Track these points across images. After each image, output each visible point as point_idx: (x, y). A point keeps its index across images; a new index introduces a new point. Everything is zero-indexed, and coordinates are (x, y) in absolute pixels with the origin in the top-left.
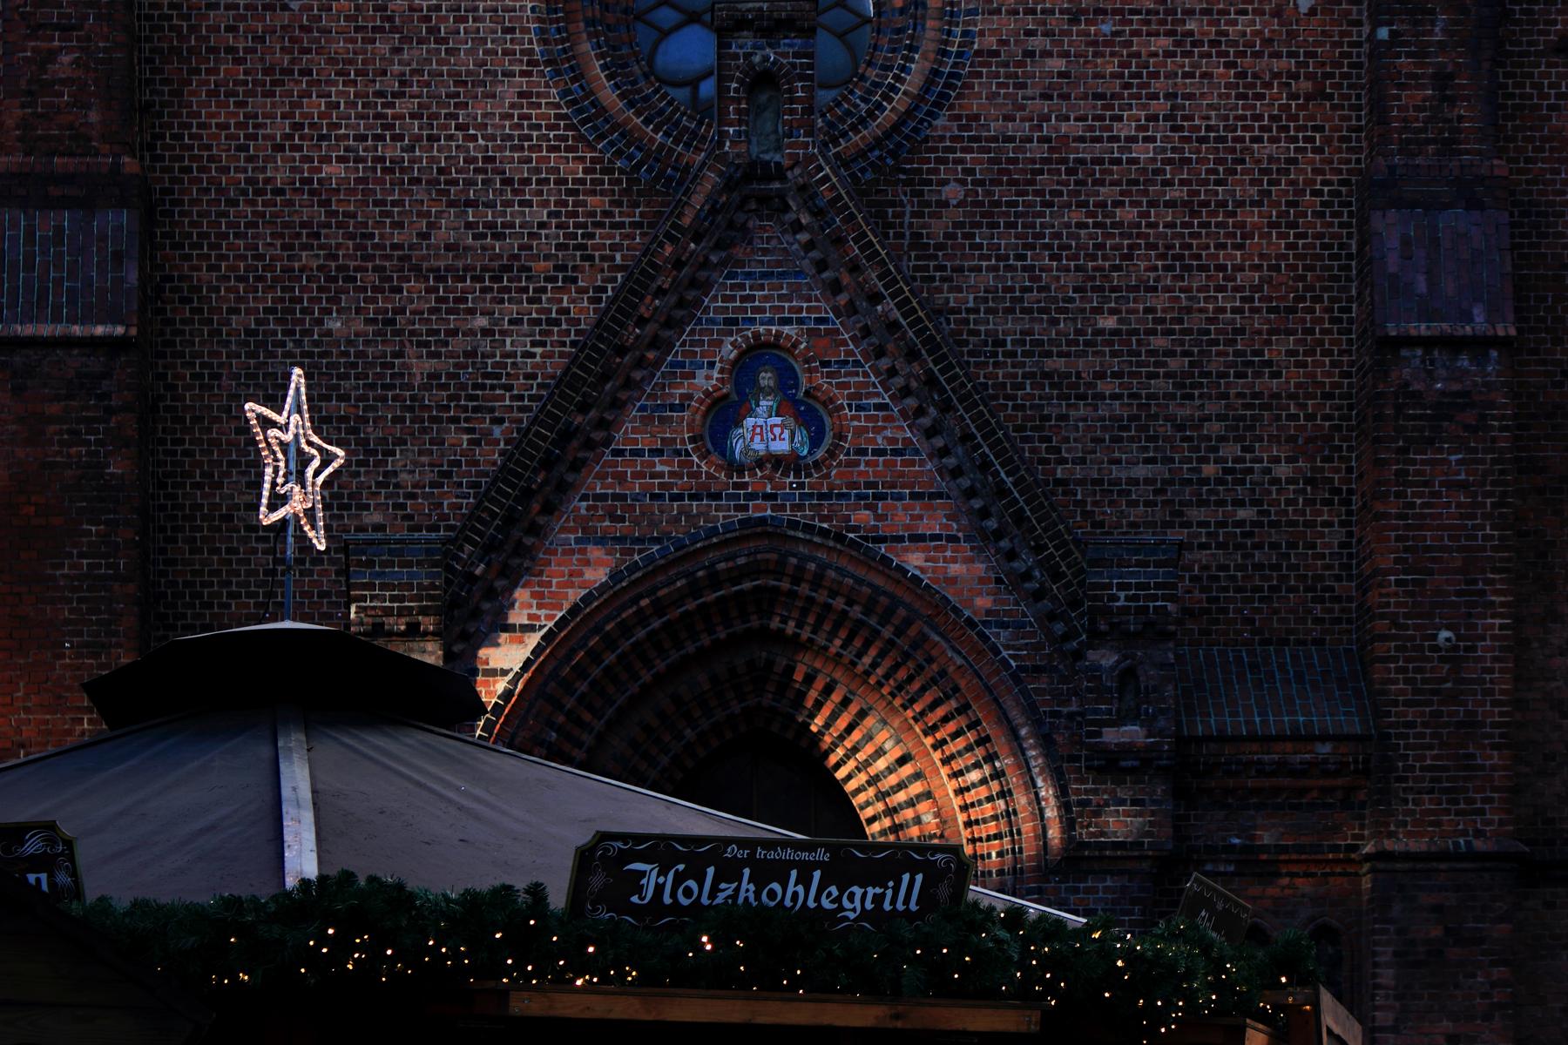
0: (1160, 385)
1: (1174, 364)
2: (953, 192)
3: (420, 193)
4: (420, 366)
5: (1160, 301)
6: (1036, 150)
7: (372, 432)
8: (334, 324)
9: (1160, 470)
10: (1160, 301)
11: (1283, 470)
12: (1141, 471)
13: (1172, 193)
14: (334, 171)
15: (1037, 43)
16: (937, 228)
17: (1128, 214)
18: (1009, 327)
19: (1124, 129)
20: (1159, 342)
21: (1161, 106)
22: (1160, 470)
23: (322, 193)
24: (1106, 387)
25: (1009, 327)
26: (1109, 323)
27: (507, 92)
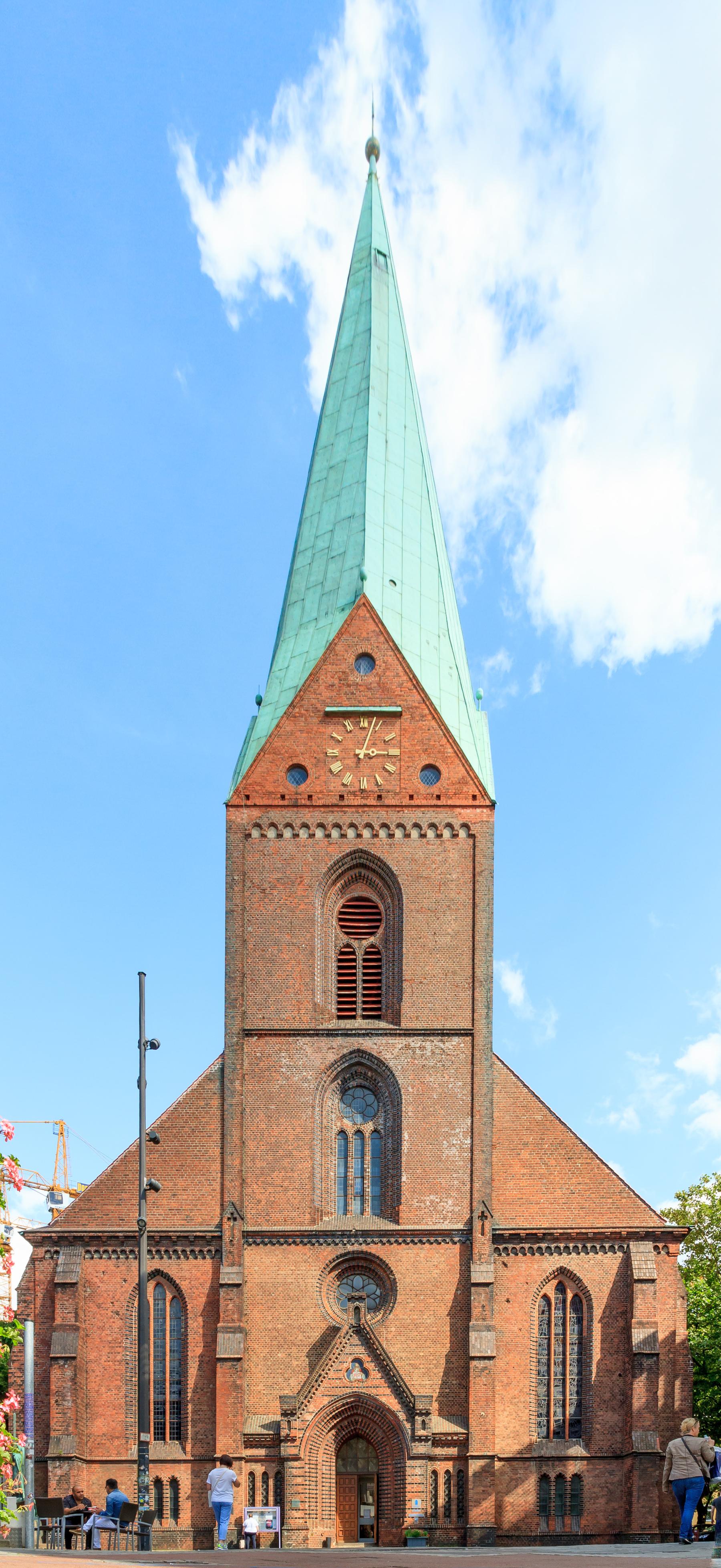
0: (432, 1366)
1: (435, 1362)
2: (393, 1329)
3: (295, 1330)
4: (295, 1363)
5: (431, 1350)
6: (409, 1321)
7: (286, 1375)
8: (279, 1355)
9: (431, 1382)
10: (431, 1350)
11: (454, 1382)
12: (428, 1382)
13: (435, 1329)
14: (280, 1326)
15: (409, 1301)
16: (390, 1336)
17: (426, 1333)
18: (403, 1355)
19: (425, 1317)
20: (431, 1358)
21: (432, 1313)
22: (431, 1382)
23: (277, 1331)
24: (422, 1366)
25: (403, 1355)
26: (422, 1354)
27: (311, 1311)
